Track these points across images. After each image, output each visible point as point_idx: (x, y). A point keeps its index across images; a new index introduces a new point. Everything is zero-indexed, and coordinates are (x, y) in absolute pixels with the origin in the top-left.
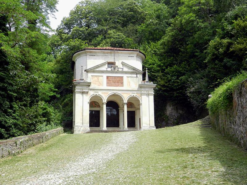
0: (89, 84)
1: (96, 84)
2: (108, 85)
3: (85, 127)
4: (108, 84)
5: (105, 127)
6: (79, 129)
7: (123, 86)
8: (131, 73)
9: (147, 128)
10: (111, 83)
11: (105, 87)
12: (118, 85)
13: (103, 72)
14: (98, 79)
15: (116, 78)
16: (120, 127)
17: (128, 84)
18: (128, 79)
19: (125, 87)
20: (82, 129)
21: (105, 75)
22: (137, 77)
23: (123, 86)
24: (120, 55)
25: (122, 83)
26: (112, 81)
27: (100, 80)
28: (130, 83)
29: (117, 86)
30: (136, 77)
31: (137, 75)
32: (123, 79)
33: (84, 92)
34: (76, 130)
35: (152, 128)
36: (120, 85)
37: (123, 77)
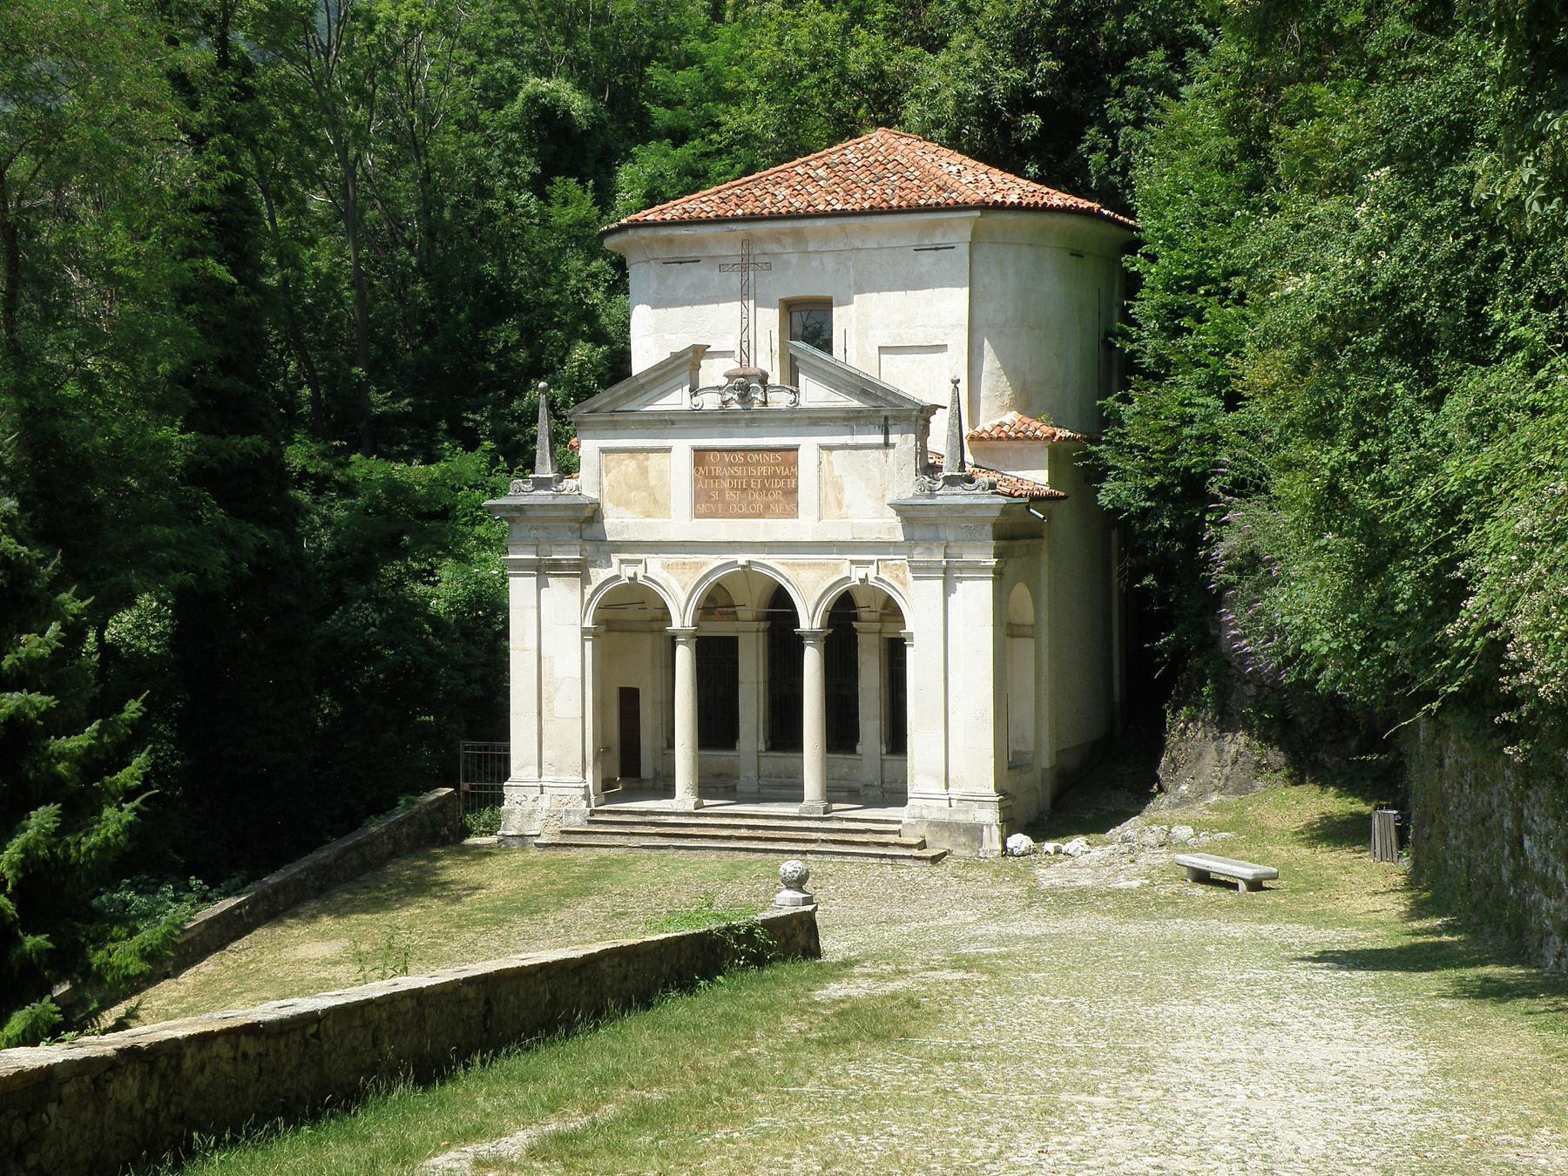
0: (587, 513)
1: (628, 504)
2: (703, 508)
3: (565, 791)
4: (706, 502)
5: (684, 798)
6: (529, 806)
7: (793, 513)
8: (845, 419)
9: (940, 809)
10: (721, 492)
11: (680, 523)
12: (767, 507)
13: (673, 423)
14: (644, 471)
15: (755, 456)
16: (859, 748)
17: (831, 498)
18: (830, 463)
19: (802, 527)
20: (545, 803)
21: (682, 448)
22: (887, 445)
23: (793, 513)
24: (858, 244)
25: (792, 493)
26: (726, 485)
27: (652, 474)
28: (841, 490)
29: (760, 516)
30: (877, 447)
31: (887, 433)
32: (796, 463)
33: (556, 565)
34: (511, 812)
35: (976, 805)
36: (776, 508)
37: (795, 449)
